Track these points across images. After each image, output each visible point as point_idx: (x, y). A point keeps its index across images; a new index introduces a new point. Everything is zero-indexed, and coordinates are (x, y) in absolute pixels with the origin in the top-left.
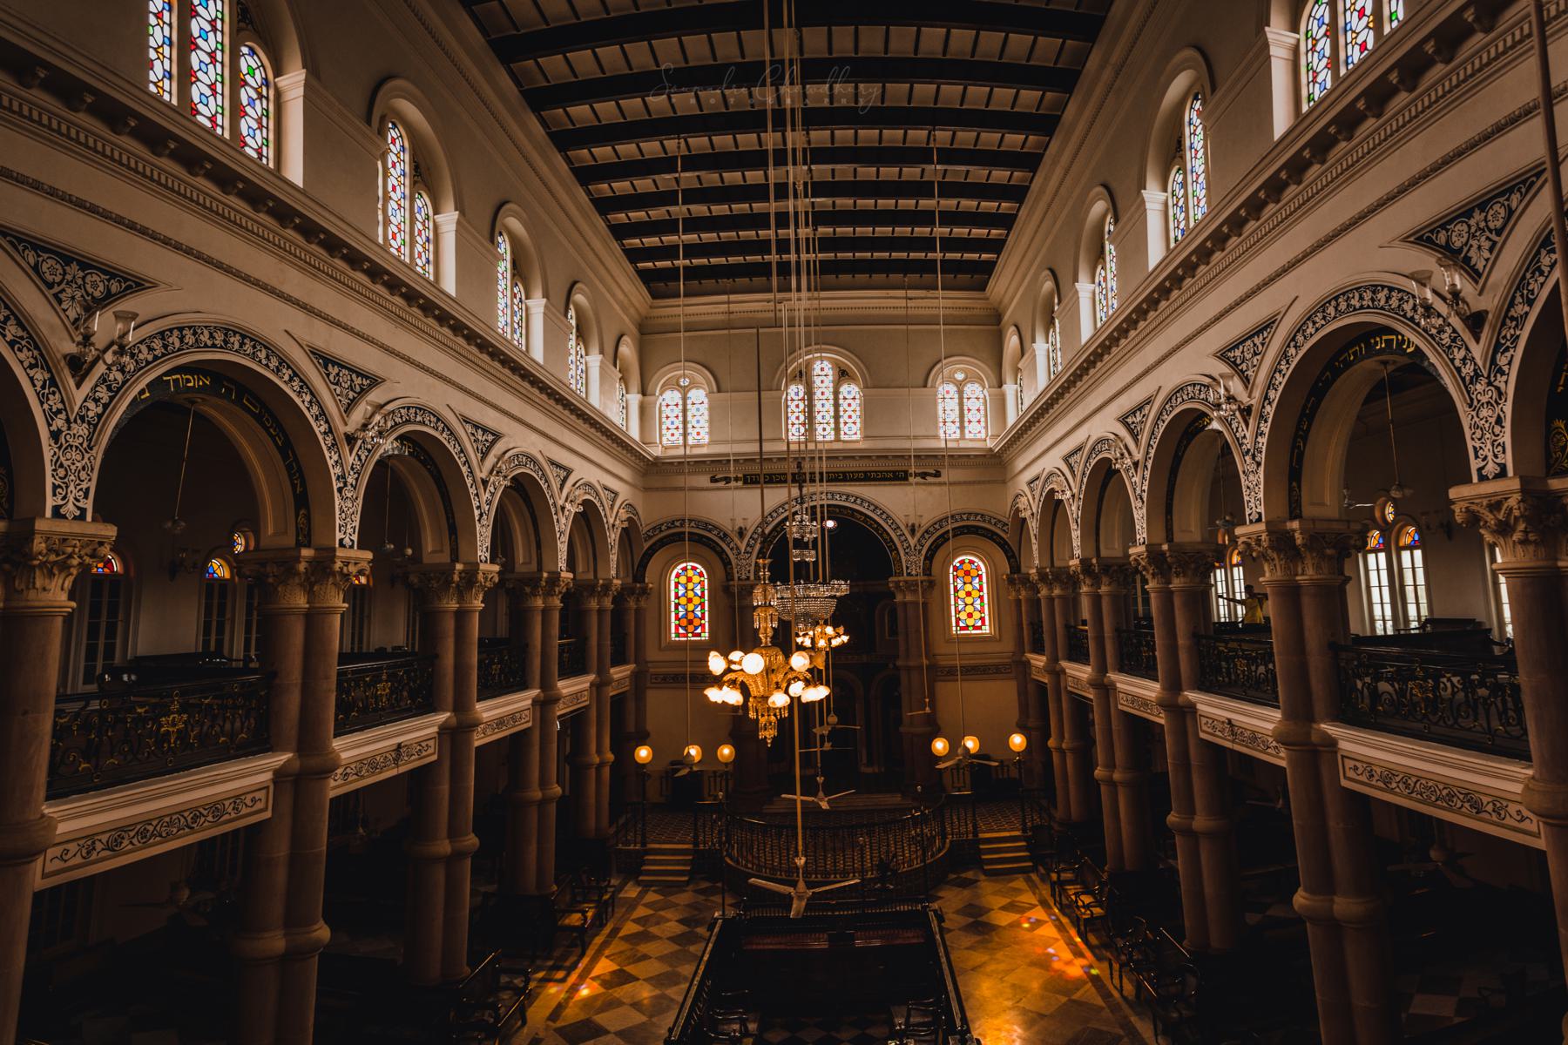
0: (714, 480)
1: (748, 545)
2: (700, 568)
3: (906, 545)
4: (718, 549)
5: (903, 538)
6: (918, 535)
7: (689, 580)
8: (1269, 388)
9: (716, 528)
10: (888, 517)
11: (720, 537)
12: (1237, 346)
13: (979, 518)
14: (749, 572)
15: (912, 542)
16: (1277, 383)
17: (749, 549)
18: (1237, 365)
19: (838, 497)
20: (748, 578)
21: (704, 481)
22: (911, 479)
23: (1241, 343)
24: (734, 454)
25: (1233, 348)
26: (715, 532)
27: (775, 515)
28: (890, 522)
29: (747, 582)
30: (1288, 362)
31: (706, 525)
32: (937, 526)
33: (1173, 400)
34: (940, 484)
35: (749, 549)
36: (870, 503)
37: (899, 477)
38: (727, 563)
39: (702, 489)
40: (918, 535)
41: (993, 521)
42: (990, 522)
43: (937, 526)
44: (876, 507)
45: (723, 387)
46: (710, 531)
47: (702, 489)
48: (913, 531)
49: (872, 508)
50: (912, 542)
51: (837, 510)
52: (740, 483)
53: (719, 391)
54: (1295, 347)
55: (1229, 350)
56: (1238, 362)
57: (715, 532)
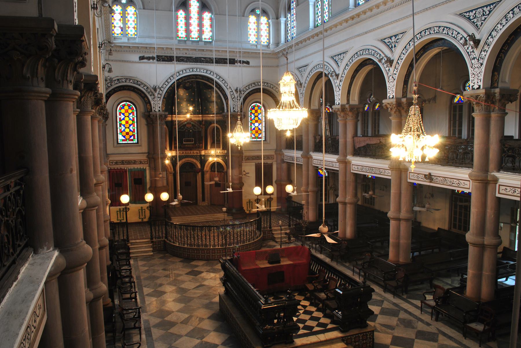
0: (142, 58)
3: (233, 97)
4: (143, 95)
5: (232, 93)
7: (127, 111)
8: (493, 31)
9: (142, 84)
12: (472, 11)
16: (498, 29)
17: (159, 96)
18: (470, 20)
19: (202, 71)
21: (135, 57)
23: (475, 10)
24: (157, 45)
25: (469, 12)
26: (142, 86)
30: (507, 20)
31: (137, 82)
32: (247, 88)
33: (423, 33)
34: (249, 66)
35: (159, 96)
36: (217, 75)
37: (233, 62)
38: (147, 102)
39: (136, 62)
41: (272, 86)
42: (270, 87)
44: (220, 77)
45: (146, 7)
46: (139, 85)
47: (136, 62)
49: (218, 77)
51: (195, 77)
53: (144, 9)
54: (513, 14)
55: (466, 12)
56: (471, 18)
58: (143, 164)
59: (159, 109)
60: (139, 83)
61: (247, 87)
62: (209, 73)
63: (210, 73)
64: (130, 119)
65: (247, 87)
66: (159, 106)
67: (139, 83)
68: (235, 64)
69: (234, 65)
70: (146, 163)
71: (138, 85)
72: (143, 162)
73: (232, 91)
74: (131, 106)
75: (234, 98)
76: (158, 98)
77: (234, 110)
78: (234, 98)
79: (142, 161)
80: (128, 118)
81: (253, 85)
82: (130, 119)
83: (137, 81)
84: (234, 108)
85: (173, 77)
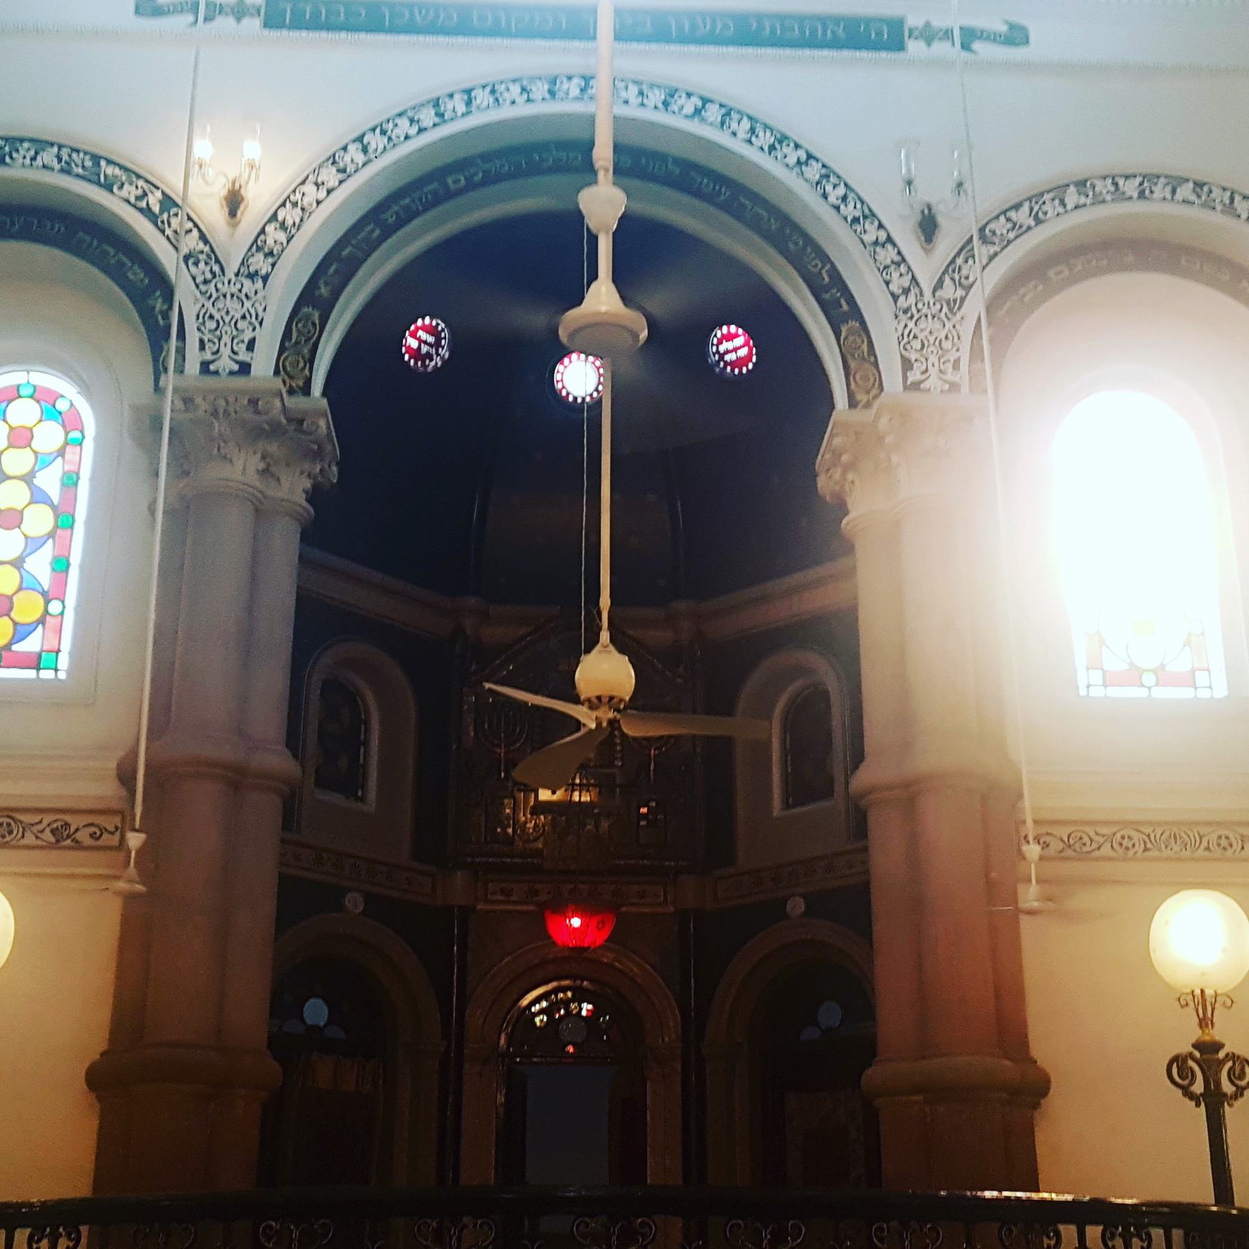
1: (257, 245)
2: (69, 393)
6: (946, 245)
10: (828, 173)
11: (147, 212)
13: (1185, 191)
14: (251, 345)
15: (926, 267)
17: (260, 263)
20: (245, 368)
22: (915, 47)
26: (130, 192)
27: (377, 141)
28: (835, 195)
29: (240, 382)
40: (946, 245)
43: (1022, 216)
44: (782, 139)
46: (109, 188)
48: (928, 227)
50: (926, 267)
52: (253, 24)
57: (130, 192)
58: (78, 846)
59: (243, 356)
60: (110, 170)
61: (1017, 207)
62: (689, 109)
63: (697, 112)
64: (38, 497)
65: (1017, 207)
66: (247, 336)
67: (110, 170)
68: (901, 47)
69: (901, 55)
70: (107, 839)
71: (99, 184)
72: (83, 836)
73: (889, 239)
74: (62, 405)
75: (906, 291)
76: (252, 276)
77: (914, 376)
78: (906, 291)
79: (75, 821)
80: (23, 485)
81: (1072, 198)
82: (38, 497)
83: (96, 159)
84: (907, 365)
85: (383, 132)
